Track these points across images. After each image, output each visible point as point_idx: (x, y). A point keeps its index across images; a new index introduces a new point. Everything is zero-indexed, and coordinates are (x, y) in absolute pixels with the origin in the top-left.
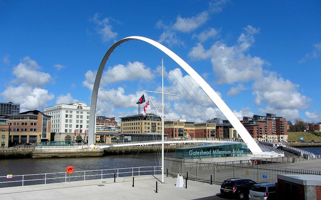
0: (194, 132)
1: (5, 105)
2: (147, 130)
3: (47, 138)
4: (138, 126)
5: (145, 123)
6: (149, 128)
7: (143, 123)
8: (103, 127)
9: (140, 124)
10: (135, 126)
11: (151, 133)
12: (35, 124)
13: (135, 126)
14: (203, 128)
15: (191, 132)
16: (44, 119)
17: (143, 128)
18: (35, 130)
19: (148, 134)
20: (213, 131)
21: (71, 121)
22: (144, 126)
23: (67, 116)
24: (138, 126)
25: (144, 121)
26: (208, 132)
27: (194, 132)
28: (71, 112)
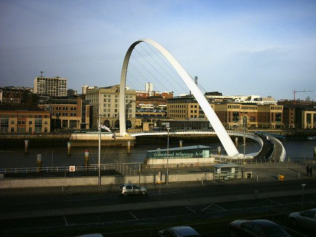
0: (256, 115)
1: (52, 80)
2: (194, 114)
3: (86, 123)
4: (184, 109)
5: (192, 107)
6: (196, 112)
7: (189, 106)
8: (152, 106)
9: (186, 107)
10: (179, 109)
11: (198, 119)
12: (75, 109)
13: (179, 109)
14: (267, 111)
15: (252, 115)
16: (83, 104)
17: (189, 112)
18: (75, 115)
19: (193, 119)
20: (278, 115)
21: (109, 105)
22: (190, 109)
23: (105, 100)
24: (184, 109)
25: (190, 104)
26: (272, 115)
27: (256, 115)
28: (109, 96)
